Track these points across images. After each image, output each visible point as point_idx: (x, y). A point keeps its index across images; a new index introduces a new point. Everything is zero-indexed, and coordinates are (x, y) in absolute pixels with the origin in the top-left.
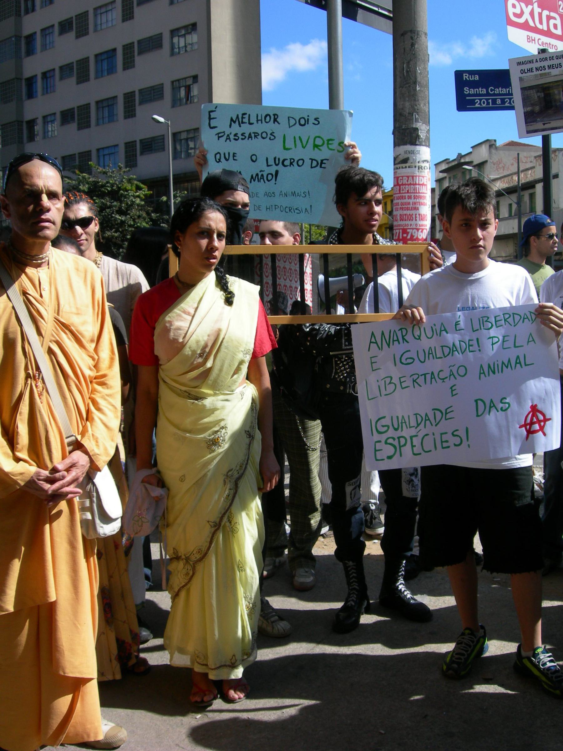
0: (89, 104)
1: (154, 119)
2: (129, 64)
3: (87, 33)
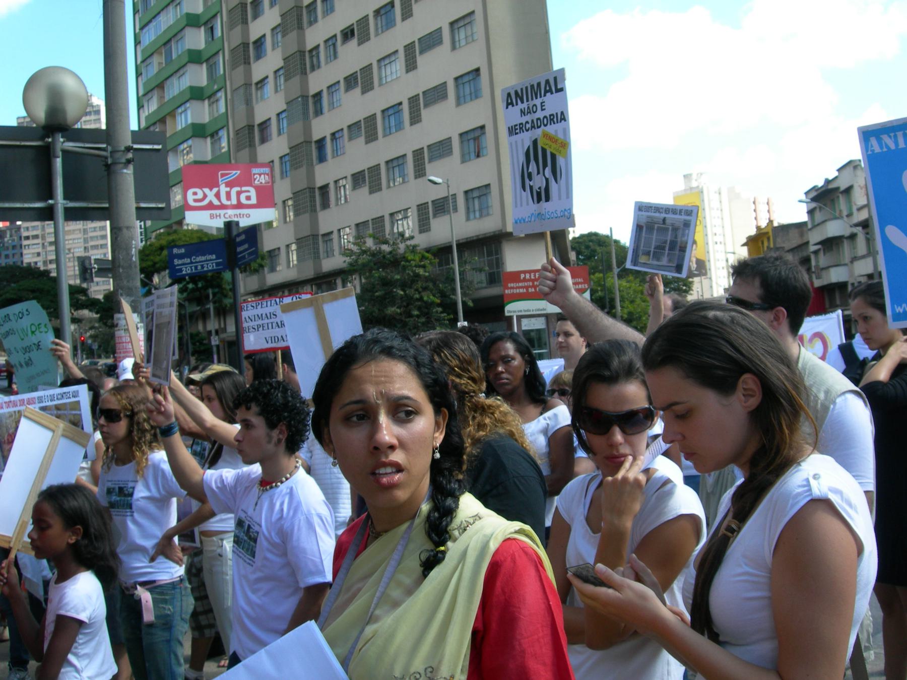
0: (379, 164)
1: (430, 181)
2: (415, 118)
3: (372, 88)
